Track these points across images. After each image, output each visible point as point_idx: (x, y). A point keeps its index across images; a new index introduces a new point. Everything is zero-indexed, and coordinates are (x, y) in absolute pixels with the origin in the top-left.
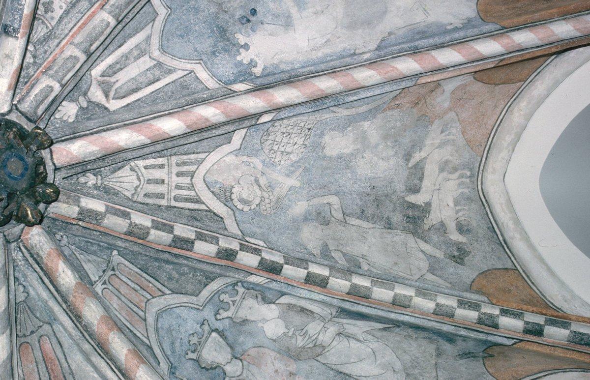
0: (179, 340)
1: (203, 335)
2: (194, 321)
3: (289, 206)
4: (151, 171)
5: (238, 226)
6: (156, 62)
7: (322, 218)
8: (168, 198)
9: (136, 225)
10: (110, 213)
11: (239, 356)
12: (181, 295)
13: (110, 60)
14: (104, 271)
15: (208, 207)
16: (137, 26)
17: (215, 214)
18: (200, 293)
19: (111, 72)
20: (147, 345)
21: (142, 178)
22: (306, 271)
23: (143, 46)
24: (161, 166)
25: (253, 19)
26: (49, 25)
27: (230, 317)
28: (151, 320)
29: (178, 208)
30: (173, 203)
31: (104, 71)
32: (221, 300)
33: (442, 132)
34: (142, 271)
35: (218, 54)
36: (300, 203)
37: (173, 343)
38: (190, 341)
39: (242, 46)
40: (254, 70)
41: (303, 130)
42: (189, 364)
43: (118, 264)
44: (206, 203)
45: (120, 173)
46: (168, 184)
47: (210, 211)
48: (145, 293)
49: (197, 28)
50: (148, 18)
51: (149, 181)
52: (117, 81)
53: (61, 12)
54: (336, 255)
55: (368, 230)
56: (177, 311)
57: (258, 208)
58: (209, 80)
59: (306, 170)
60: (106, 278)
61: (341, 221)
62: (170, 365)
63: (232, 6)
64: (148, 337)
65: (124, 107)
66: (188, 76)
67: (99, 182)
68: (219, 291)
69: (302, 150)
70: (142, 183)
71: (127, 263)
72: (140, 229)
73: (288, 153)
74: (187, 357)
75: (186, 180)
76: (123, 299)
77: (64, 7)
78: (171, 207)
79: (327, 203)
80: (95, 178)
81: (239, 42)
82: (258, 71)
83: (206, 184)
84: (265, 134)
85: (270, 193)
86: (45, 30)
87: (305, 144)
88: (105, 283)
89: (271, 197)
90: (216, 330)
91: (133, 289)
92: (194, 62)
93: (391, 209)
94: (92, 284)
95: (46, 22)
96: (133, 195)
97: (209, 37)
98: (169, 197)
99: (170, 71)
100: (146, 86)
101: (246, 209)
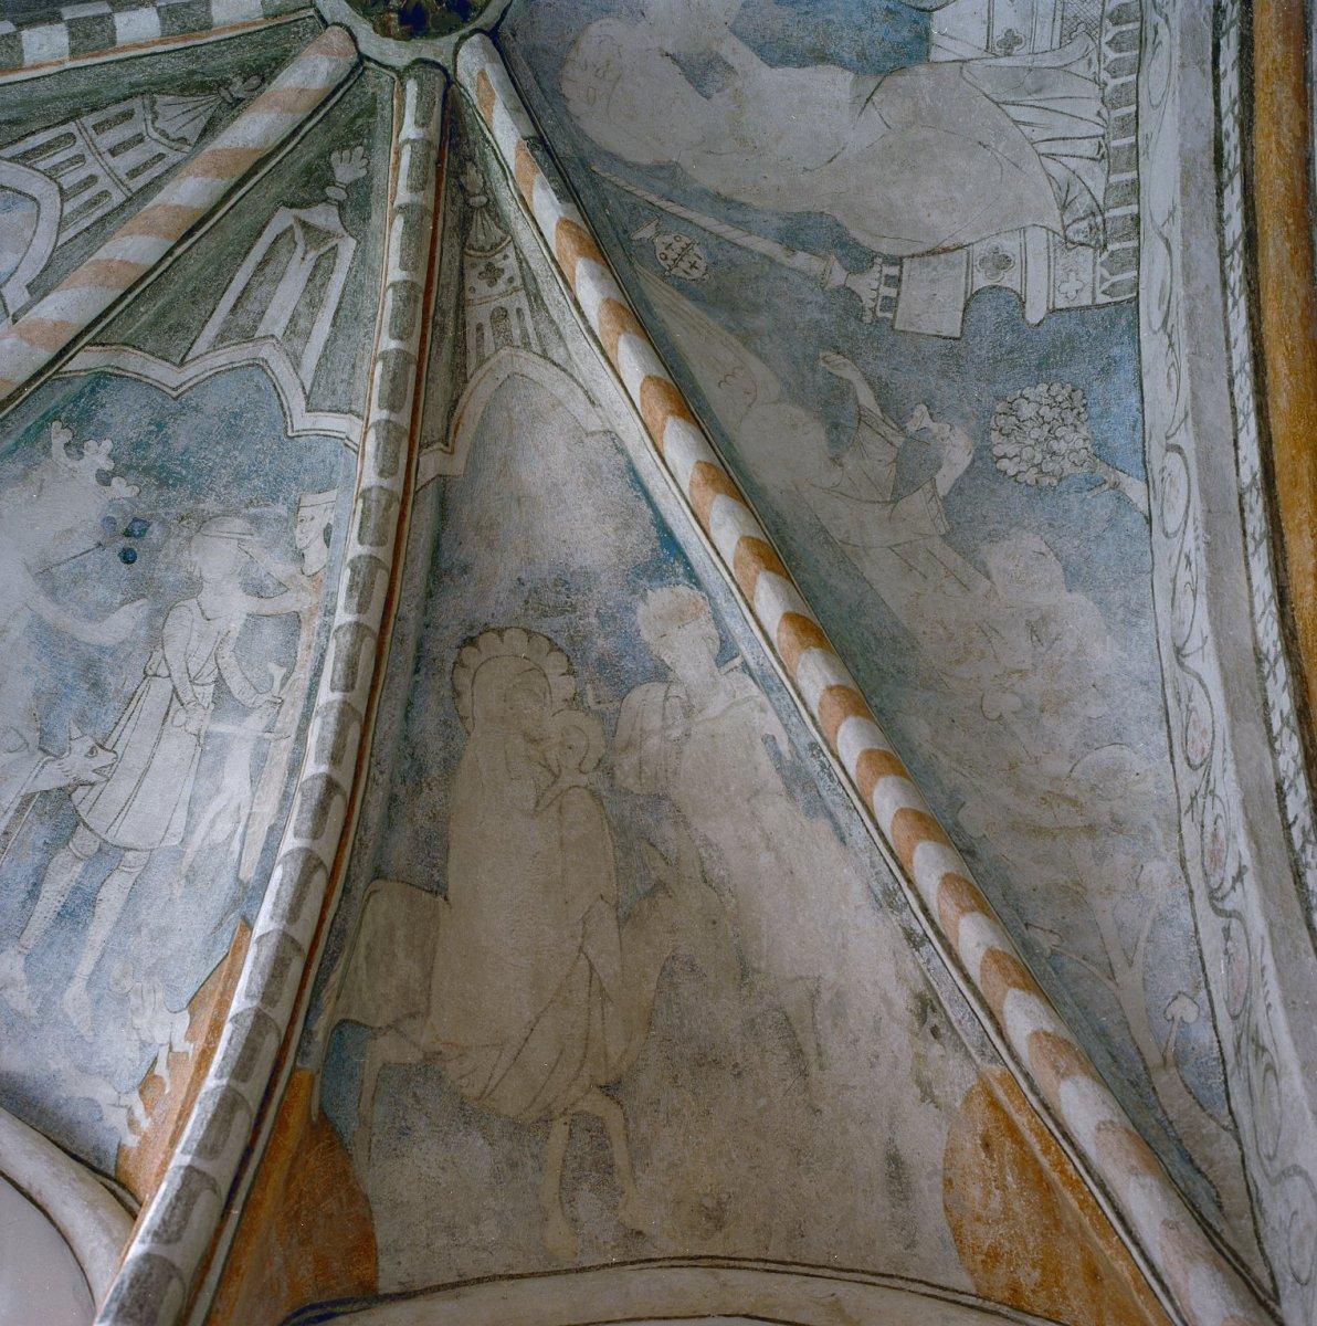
4: (147, 157)
13: (338, 279)
16: (332, 363)
19: (325, 264)
21: (156, 135)
23: (297, 342)
24: (133, 173)
25: (124, 542)
26: (472, 252)
30: (71, 127)
31: (335, 256)
39: (114, 473)
40: (66, 436)
45: (201, 123)
49: (220, 449)
51: (139, 139)
53: (467, 286)
58: (142, 367)
65: (264, 227)
67: (224, 93)
70: (151, 130)
75: (70, 179)
77: (469, 295)
78: (72, 119)
82: (59, 436)
83: (26, 195)
86: (471, 241)
92: (185, 387)
95: (479, 254)
96: (154, 103)
97: (186, 450)
98: (85, 134)
99: (221, 338)
100: (248, 284)
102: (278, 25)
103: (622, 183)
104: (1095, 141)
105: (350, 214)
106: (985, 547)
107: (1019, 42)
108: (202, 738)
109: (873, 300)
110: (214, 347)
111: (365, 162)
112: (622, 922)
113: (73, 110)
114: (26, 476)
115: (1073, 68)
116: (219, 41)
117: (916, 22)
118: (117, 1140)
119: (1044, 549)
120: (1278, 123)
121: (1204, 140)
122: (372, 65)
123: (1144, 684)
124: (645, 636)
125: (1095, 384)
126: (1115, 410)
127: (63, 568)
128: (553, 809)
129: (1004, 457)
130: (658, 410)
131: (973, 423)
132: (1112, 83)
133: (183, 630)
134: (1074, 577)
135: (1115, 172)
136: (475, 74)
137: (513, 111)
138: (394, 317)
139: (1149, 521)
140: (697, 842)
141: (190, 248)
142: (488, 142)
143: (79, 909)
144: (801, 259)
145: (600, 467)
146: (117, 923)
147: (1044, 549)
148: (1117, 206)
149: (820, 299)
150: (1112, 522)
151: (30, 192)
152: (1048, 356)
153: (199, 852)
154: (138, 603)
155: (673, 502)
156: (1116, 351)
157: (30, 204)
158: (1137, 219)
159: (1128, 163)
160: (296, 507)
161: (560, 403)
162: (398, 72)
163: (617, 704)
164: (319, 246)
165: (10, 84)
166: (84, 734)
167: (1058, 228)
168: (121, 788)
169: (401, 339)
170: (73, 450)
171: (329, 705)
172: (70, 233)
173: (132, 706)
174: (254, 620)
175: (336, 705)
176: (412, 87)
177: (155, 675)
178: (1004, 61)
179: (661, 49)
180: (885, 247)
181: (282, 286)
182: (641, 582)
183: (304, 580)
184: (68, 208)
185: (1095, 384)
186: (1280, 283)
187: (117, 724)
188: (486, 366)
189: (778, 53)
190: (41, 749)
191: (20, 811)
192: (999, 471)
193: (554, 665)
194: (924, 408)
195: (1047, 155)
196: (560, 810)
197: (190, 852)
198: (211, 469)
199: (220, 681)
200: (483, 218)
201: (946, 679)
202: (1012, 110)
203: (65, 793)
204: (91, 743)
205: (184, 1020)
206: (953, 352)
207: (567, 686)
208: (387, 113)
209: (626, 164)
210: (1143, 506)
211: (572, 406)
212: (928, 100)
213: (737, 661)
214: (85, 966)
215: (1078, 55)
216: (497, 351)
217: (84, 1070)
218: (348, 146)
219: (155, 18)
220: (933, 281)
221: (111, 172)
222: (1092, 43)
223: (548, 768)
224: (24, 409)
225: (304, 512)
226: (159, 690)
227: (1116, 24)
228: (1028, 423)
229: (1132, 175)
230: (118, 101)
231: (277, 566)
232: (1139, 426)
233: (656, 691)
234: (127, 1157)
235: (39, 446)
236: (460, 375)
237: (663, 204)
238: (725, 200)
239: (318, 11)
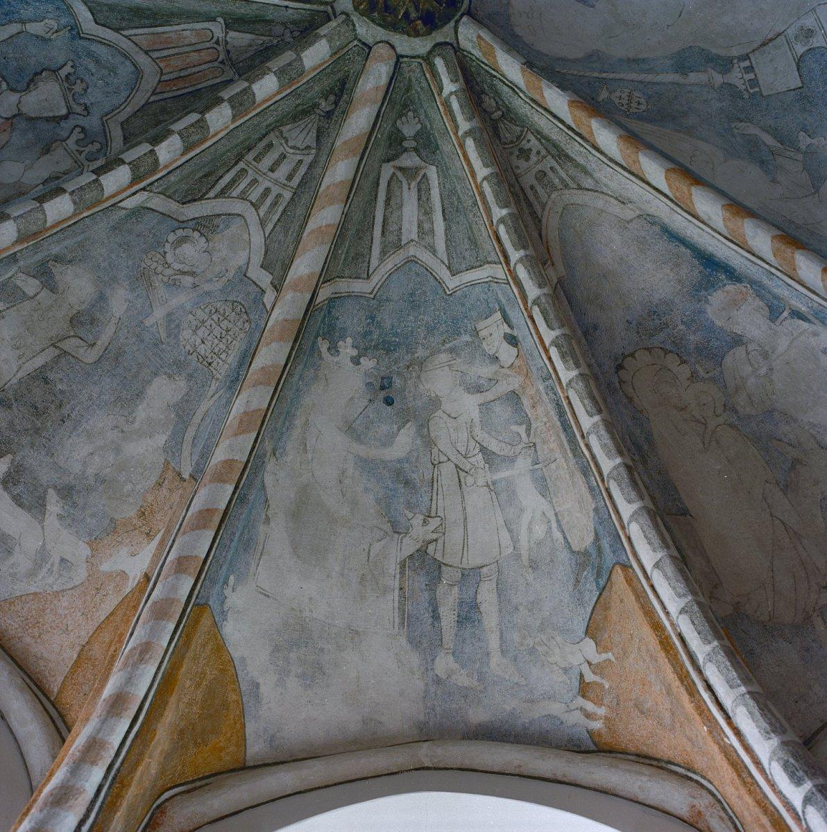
0: (94, 71)
1: (74, 100)
2: (98, 102)
3: (133, 290)
4: (293, 164)
5: (161, 213)
6: (403, 243)
7: (84, 321)
8: (251, 164)
9: (265, 74)
10: (295, 60)
11: (14, 121)
12: (136, 109)
13: (435, 193)
14: (228, 52)
15: (208, 199)
16: (455, 242)
17: (195, 200)
18: (122, 128)
19: (423, 187)
20: (123, 29)
21: (292, 151)
22: (70, 190)
23: (428, 239)
24: (290, 177)
25: (382, 394)
27: (66, 140)
28: (142, 59)
29: (232, 167)
30: (241, 165)
31: (427, 180)
32: (94, 143)
33: (63, 560)
34: (197, 90)
35: (368, 321)
36: (126, 307)
37: (97, 61)
38: (82, 82)
39: (359, 356)
41: (215, 356)
42: (61, 61)
43: (224, 71)
44: (213, 200)
45: (314, 134)
46: (264, 174)
47: (201, 199)
48: (171, 76)
49: (411, 318)
50: (455, 259)
52: (409, 189)
54: (30, 286)
55: (20, 362)
56: (125, 94)
57: (161, 251)
58: (348, 287)
59: (158, 343)
60: (220, 48)
61: (60, 340)
62: (82, 35)
63: (411, 378)
64: (130, 39)
66: (366, 269)
67: (318, 111)
68: (107, 146)
69: (188, 347)
70: (287, 149)
71: (218, 80)
72: (258, 76)
73: (197, 328)
74: (70, 63)
75: (254, 195)
76: (187, 49)
78: (240, 160)
79: (95, 344)
80: (325, 110)
81: (365, 358)
82: (323, 346)
84: (243, 310)
85: (166, 279)
87: (195, 354)
88: (217, 42)
89: (160, 276)
90: (66, 117)
91: (187, 68)
92: (376, 290)
93: (17, 421)
94: (228, 27)
95: (511, 145)
96: (281, 132)
98: (251, 166)
99: (384, 253)
101: (172, 237)
102: (339, 58)
103: (576, 72)
105: (424, 154)
108: (491, 487)
110: (382, 260)
111: (417, 119)
112: (786, 488)
113: (238, 154)
114: (317, 376)
116: (308, 81)
118: (584, 729)
122: (406, 59)
124: (718, 323)
127: (358, 422)
128: (713, 443)
130: (683, 186)
133: (441, 428)
136: (475, 39)
137: (508, 52)
138: (496, 196)
140: (807, 427)
141: (350, 205)
142: (495, 76)
143: (469, 614)
145: (645, 238)
146: (500, 610)
151: (236, 212)
153: (530, 549)
154: (408, 426)
155: (707, 237)
157: (238, 219)
160: (476, 333)
161: (602, 211)
162: (423, 58)
163: (719, 369)
164: (415, 178)
165: (203, 151)
166: (415, 514)
168: (455, 536)
169: (507, 207)
170: (333, 351)
171: (595, 425)
172: (270, 227)
173: (435, 486)
174: (485, 407)
175: (600, 423)
176: (439, 63)
177: (440, 463)
180: (735, 52)
181: (404, 210)
183: (505, 371)
184: (262, 214)
187: (431, 500)
188: (547, 208)
190: (395, 532)
191: (402, 573)
193: (671, 361)
194: (802, 133)
196: (718, 442)
197: (525, 554)
198: (412, 332)
199: (483, 450)
203: (422, 552)
204: (422, 517)
205: (589, 644)
206: (803, 96)
207: (685, 371)
208: (424, 85)
209: (575, 61)
213: (785, 314)
214: (494, 643)
216: (549, 196)
217: (532, 701)
218: (403, 115)
219: (274, 79)
220: (771, 61)
221: (276, 182)
223: (698, 421)
224: (306, 335)
225: (482, 334)
226: (447, 470)
230: (260, 139)
231: (485, 370)
233: (740, 352)
234: (600, 735)
235: (316, 355)
236: (538, 220)
237: (604, 75)
238: (634, 60)
239: (360, 41)
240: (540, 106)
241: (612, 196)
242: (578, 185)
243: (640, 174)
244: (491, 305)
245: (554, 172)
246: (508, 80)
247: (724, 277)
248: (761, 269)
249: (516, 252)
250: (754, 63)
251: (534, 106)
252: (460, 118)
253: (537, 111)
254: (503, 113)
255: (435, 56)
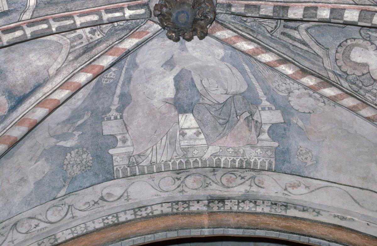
104: (156, 161)
106: (44, 159)
107: (183, 137)
109: (109, 116)
115: (175, 152)
117: (189, 110)
119: (45, 173)
120: (144, 229)
121: (145, 204)
123: (9, 214)
125: (92, 172)
126: (85, 180)
129: (71, 154)
131: (79, 144)
132: (170, 163)
134: (38, 184)
135: (147, 168)
136: (148, 31)
139: (54, 199)
142: (130, 32)
144: (116, 99)
145: (38, 75)
147: (45, 173)
148: (139, 169)
149: (106, 106)
150: (54, 188)
152: (100, 157)
156: (101, 176)
158: (135, 175)
159: (149, 171)
161: (55, 61)
167: (134, 154)
178: (178, 133)
179: (174, 55)
180: (125, 114)
182: (7, 93)
185: (92, 172)
186: (104, 238)
188: (62, 37)
189: (177, 80)
192: (67, 154)
194: (81, 133)
195: (152, 149)
200: (110, 26)
201: (2, 168)
202: (165, 138)
206: (99, 134)
209: (135, 60)
210: (59, 195)
211: (55, 64)
212: (168, 116)
215: (178, 153)
216: (68, 39)
222: (180, 156)
227: (186, 162)
228: (81, 157)
229: (146, 172)
232: (80, 189)
237: (124, 69)
240: (109, 49)
241: (61, 66)
242: (71, 53)
243: (61, 87)
244: (13, 5)
245: (80, 43)
246: (126, 38)
247: (12, 104)
248: (8, 125)
249: (30, 32)
250: (118, 120)
251: (110, 47)
252: (110, 15)
253: (108, 47)
254: (116, 27)
255: (146, 10)
